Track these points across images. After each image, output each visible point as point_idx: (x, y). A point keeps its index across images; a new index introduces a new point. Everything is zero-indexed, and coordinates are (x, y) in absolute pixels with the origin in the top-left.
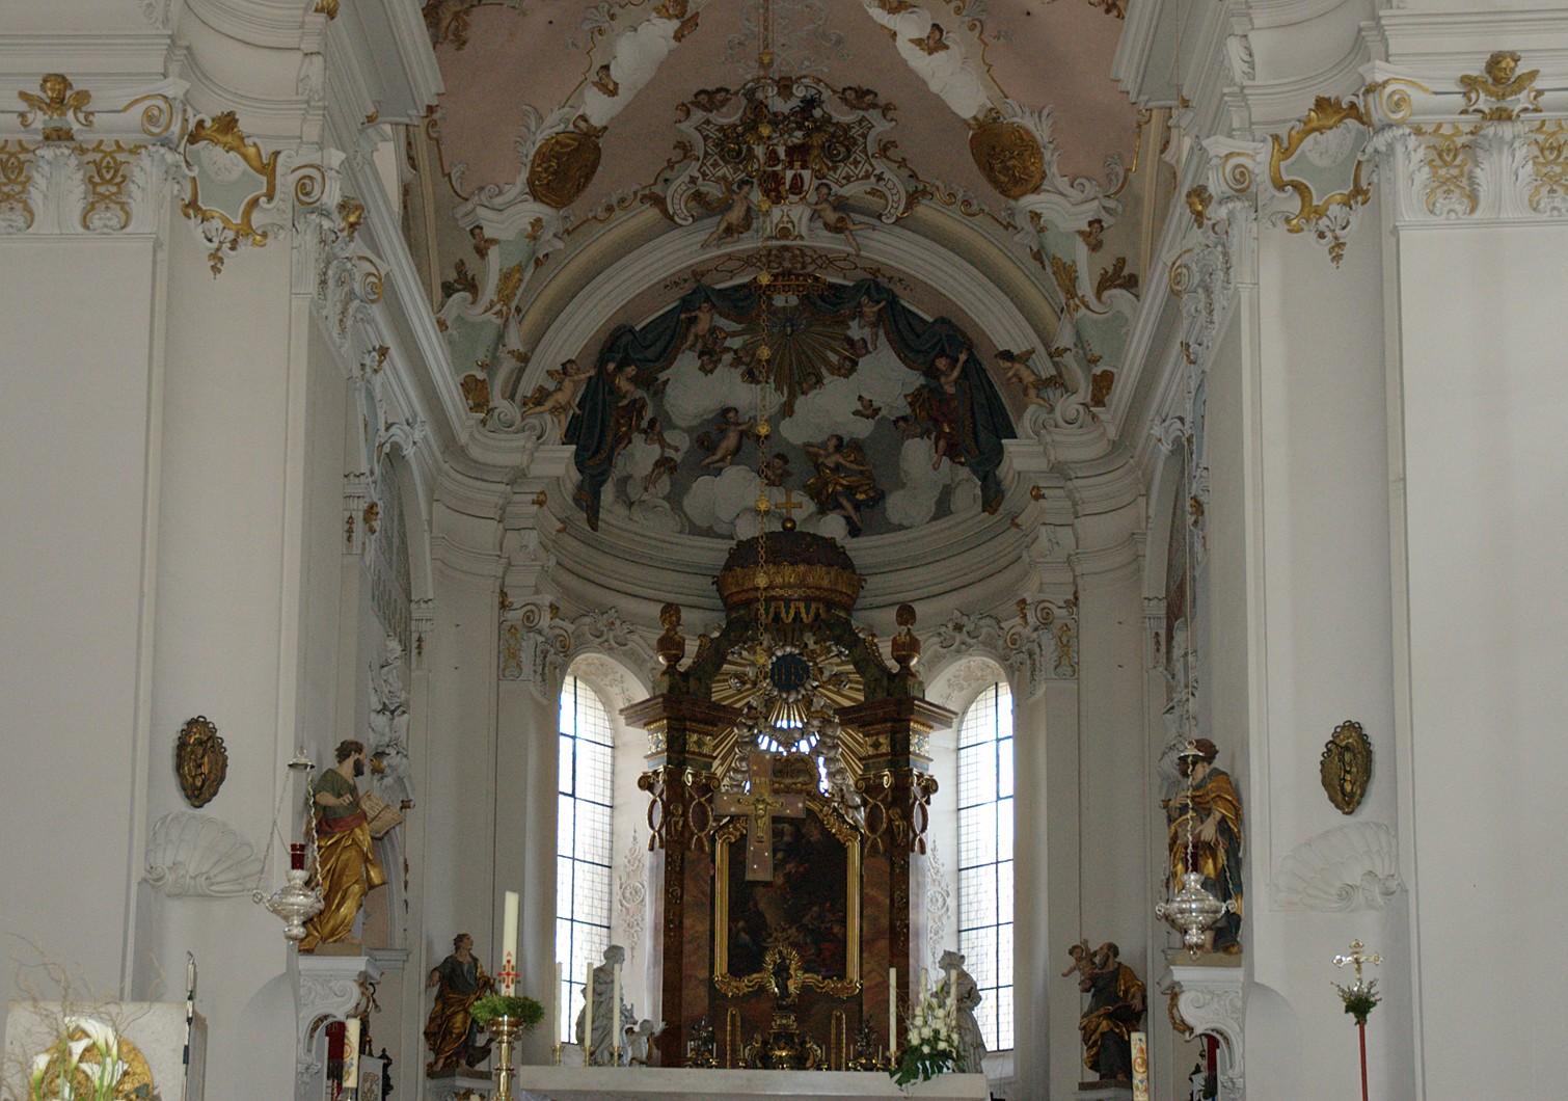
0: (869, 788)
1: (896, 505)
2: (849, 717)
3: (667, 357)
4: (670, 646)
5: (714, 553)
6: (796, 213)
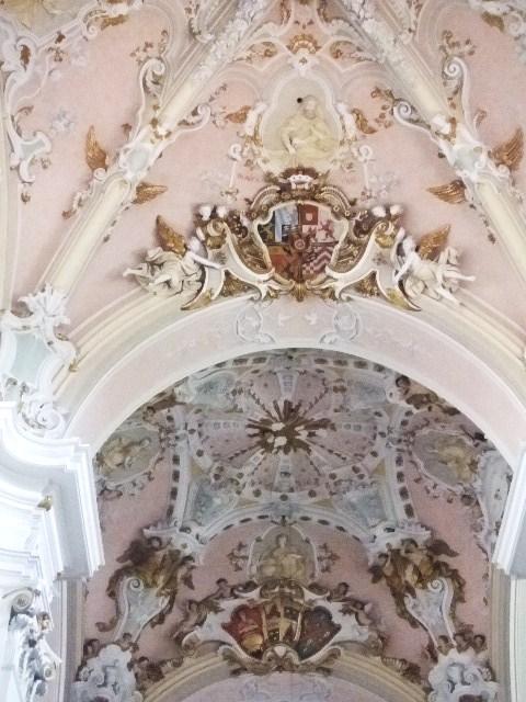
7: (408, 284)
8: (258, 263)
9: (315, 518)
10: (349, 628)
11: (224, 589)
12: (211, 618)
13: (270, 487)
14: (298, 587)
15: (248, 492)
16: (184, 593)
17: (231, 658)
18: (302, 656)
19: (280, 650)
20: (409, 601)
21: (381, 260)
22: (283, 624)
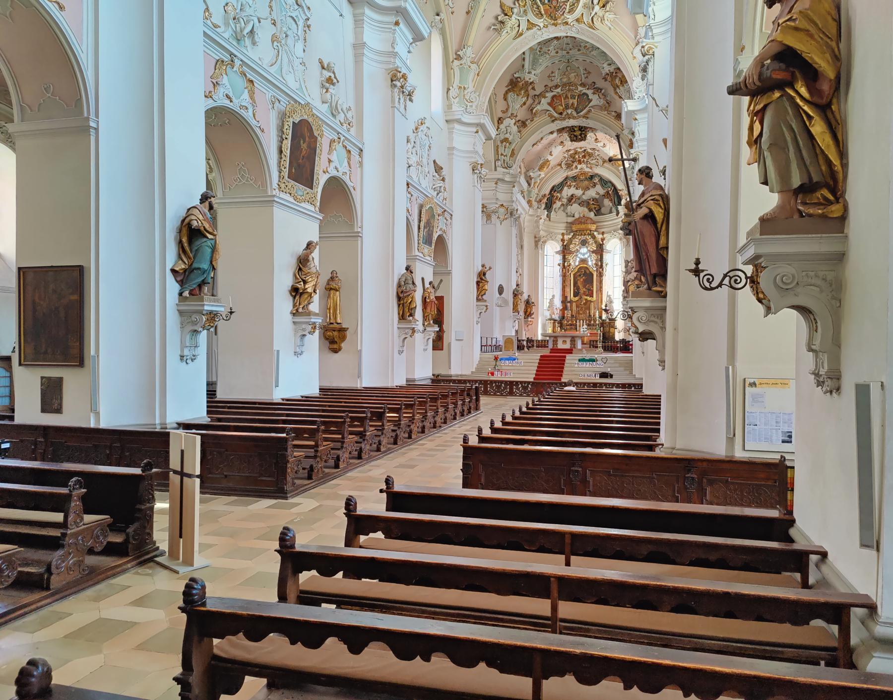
0: (596, 265)
1: (603, 210)
2: (593, 252)
3: (562, 190)
4: (563, 240)
5: (570, 220)
6: (583, 166)
7: (595, 19)
8: (540, 15)
9: (581, 59)
10: (595, 100)
11: (548, 89)
12: (543, 100)
13: (562, 49)
14: (576, 85)
15: (553, 53)
16: (532, 93)
17: (551, 116)
18: (578, 113)
19: (569, 111)
20: (618, 91)
21: (585, 6)
22: (571, 101)
